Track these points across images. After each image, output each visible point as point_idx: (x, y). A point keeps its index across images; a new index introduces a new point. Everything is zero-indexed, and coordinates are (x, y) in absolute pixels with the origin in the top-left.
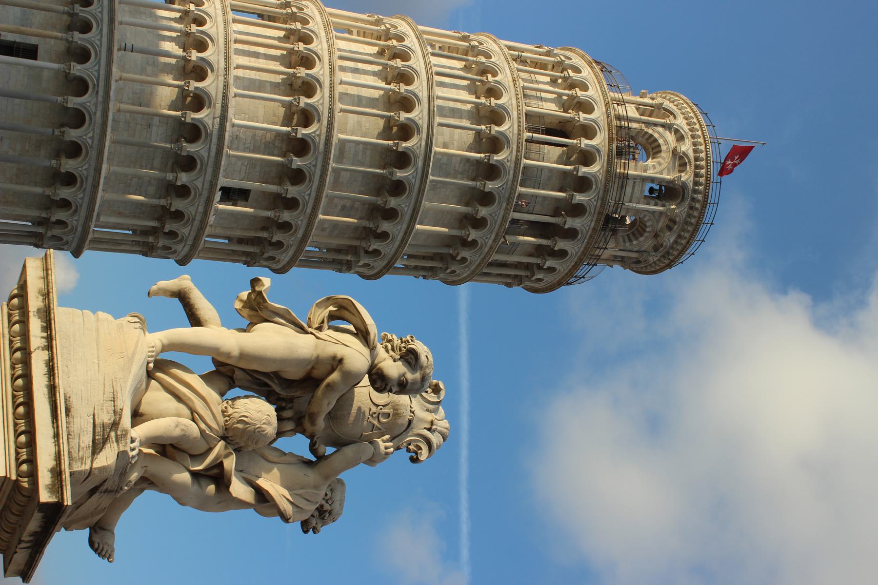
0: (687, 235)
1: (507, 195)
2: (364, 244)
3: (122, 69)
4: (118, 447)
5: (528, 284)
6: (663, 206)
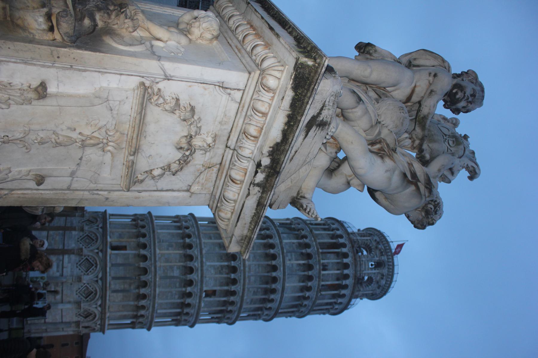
0: (389, 280)
2: (265, 305)
3: (160, 249)
5: (332, 311)
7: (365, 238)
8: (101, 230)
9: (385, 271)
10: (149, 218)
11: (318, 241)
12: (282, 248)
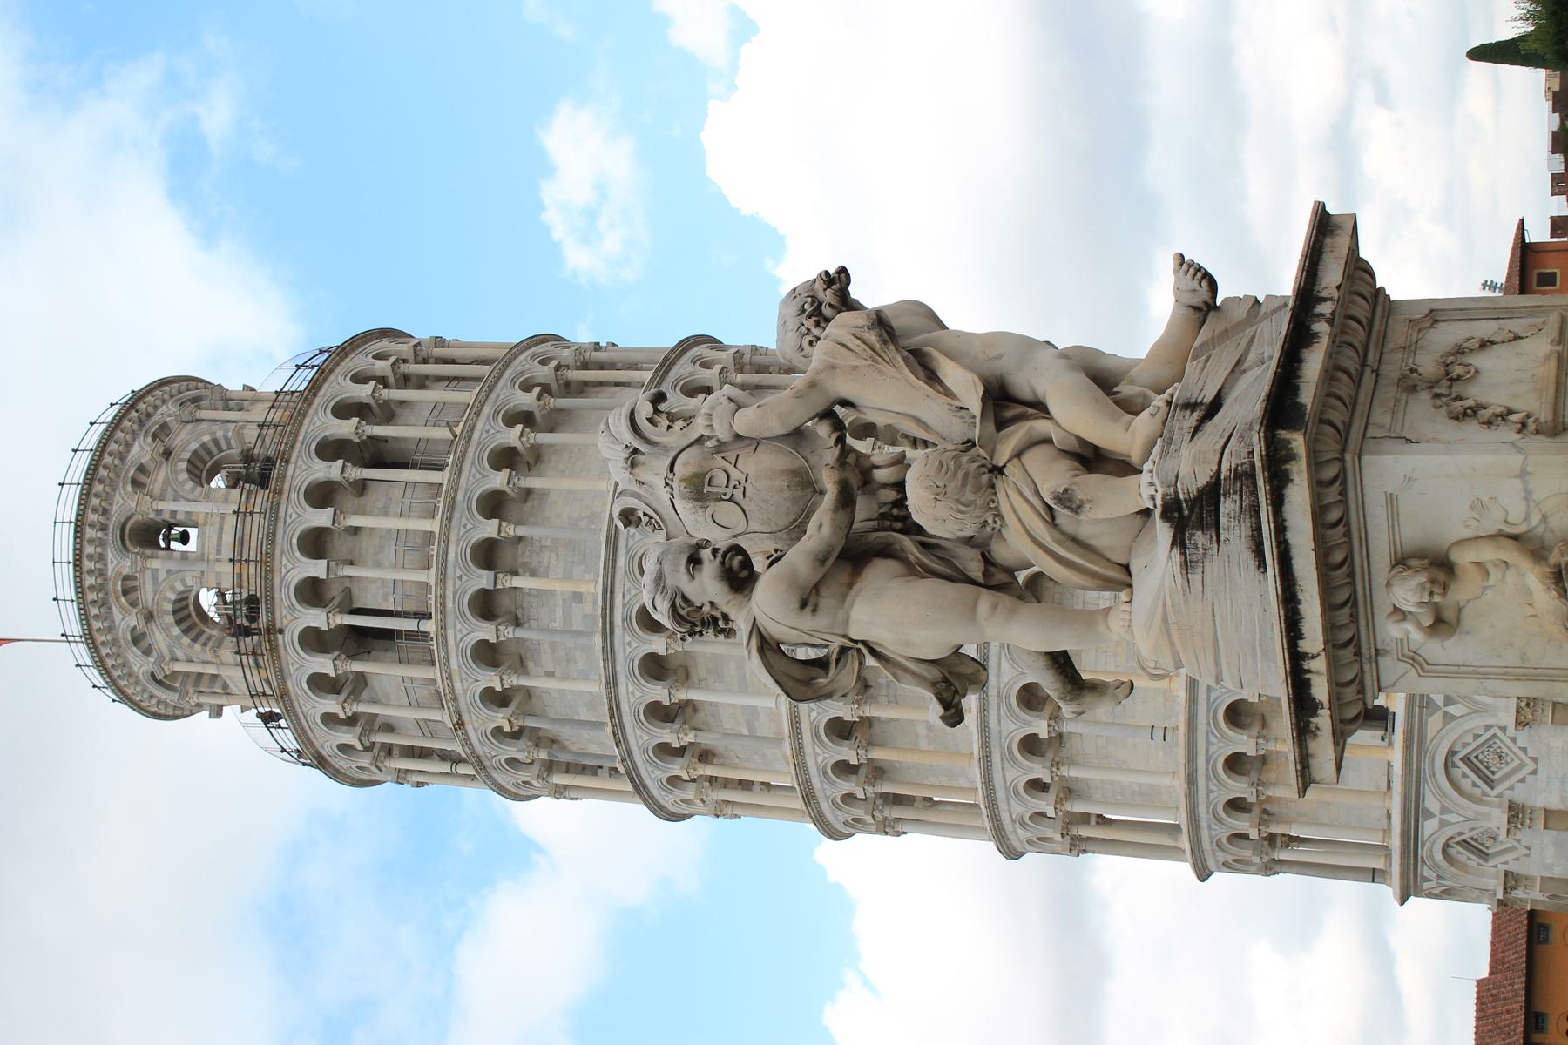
0: (107, 459)
1: (457, 514)
4: (1176, 493)
5: (405, 349)
6: (159, 512)
7: (195, 668)
8: (1431, 803)
9: (126, 504)
10: (1206, 845)
11: (434, 673)
12: (609, 654)
